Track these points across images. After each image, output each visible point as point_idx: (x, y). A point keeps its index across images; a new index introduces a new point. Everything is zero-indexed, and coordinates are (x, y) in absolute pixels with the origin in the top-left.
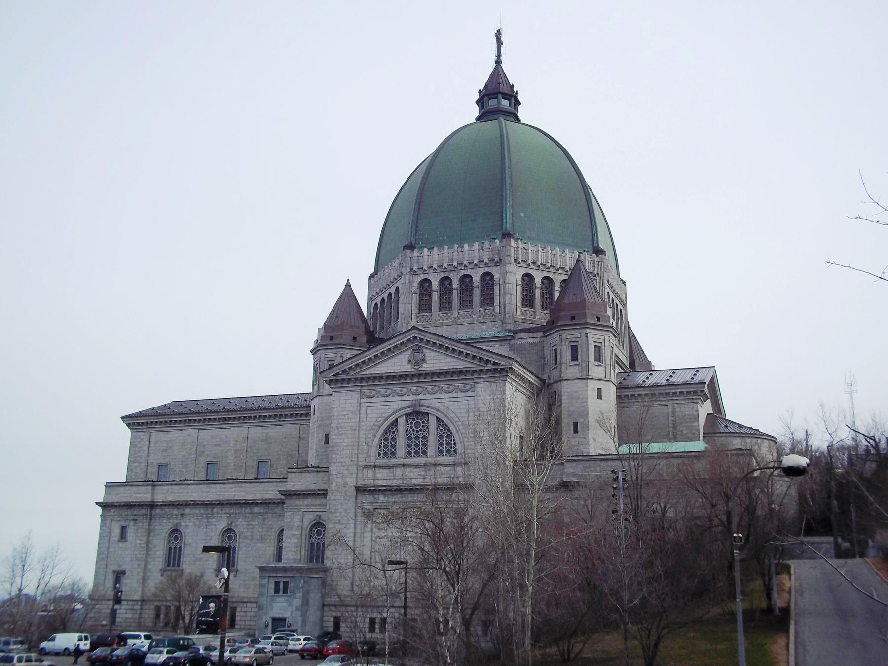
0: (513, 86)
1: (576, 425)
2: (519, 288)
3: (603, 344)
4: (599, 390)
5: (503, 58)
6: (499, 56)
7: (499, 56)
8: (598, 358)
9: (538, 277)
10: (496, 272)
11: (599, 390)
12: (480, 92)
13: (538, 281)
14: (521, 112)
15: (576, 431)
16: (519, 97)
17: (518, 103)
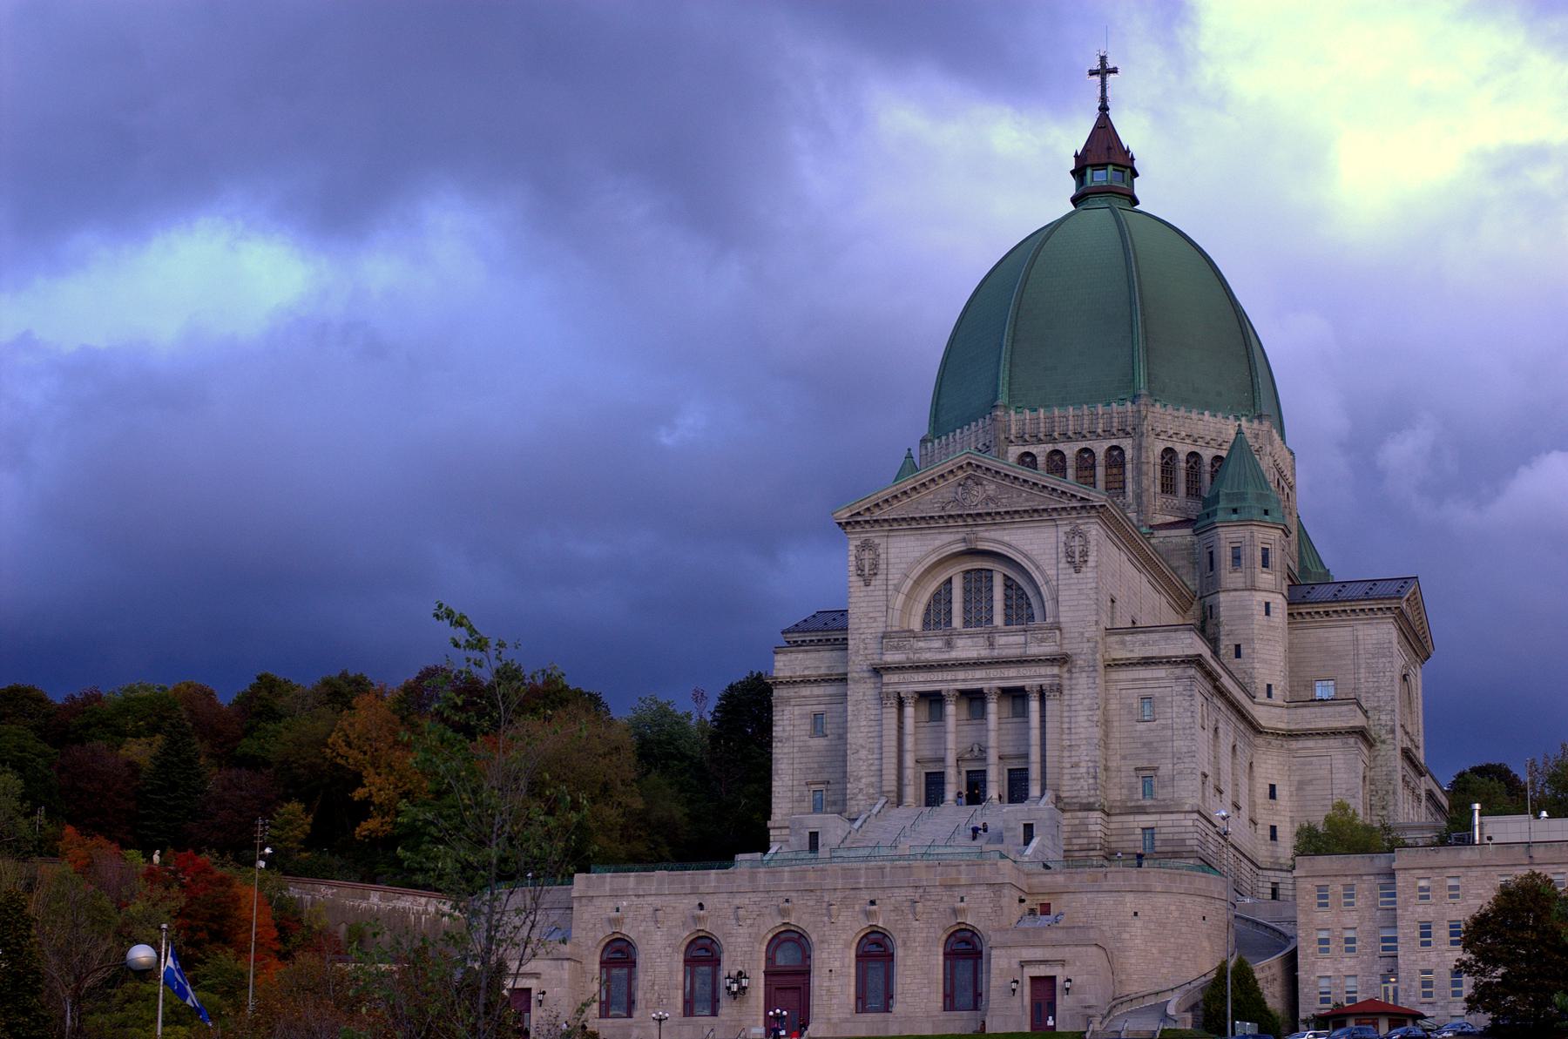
0: (1128, 151)
1: (1238, 647)
2: (1158, 468)
3: (1273, 546)
4: (1267, 604)
6: (1104, 99)
7: (1104, 99)
8: (1265, 564)
9: (1183, 450)
10: (1127, 444)
11: (1267, 604)
12: (1076, 156)
13: (1182, 457)
14: (1140, 187)
15: (1238, 655)
16: (1137, 165)
17: (1135, 174)
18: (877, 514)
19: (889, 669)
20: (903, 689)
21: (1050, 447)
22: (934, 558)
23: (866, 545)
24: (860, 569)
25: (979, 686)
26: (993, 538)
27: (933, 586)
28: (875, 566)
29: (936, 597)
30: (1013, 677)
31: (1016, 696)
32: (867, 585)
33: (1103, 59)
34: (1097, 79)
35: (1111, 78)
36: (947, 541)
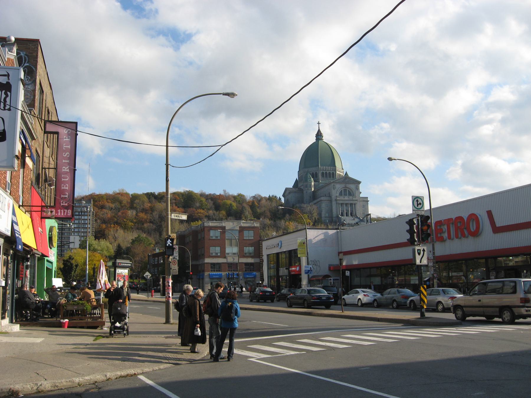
5: (320, 128)
6: (319, 127)
7: (319, 127)
18: (335, 182)
19: (338, 200)
20: (340, 202)
21: (325, 171)
22: (341, 188)
23: (334, 185)
24: (333, 188)
25: (348, 203)
26: (348, 186)
27: (341, 190)
28: (335, 187)
29: (341, 191)
30: (352, 202)
31: (351, 204)
32: (334, 190)
33: (319, 122)
34: (318, 124)
35: (320, 124)
36: (343, 185)
